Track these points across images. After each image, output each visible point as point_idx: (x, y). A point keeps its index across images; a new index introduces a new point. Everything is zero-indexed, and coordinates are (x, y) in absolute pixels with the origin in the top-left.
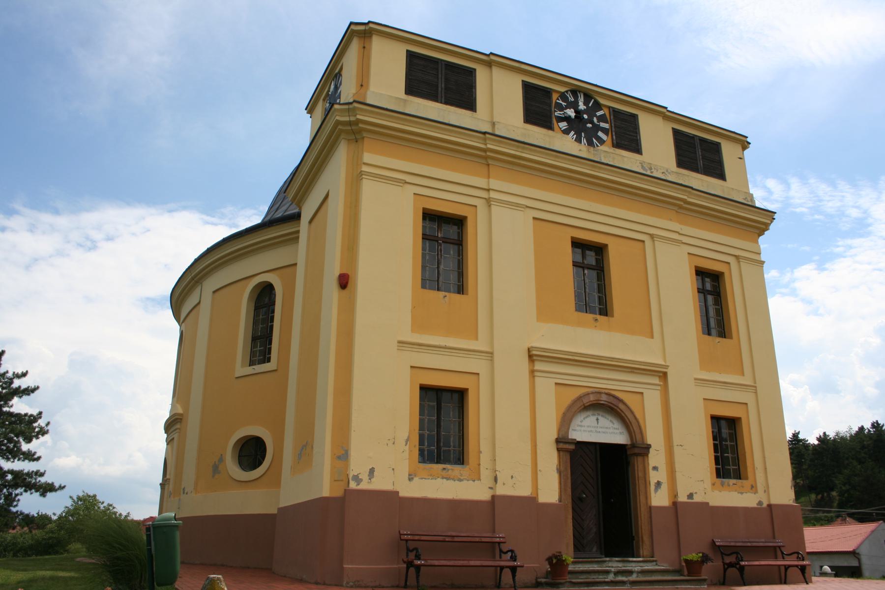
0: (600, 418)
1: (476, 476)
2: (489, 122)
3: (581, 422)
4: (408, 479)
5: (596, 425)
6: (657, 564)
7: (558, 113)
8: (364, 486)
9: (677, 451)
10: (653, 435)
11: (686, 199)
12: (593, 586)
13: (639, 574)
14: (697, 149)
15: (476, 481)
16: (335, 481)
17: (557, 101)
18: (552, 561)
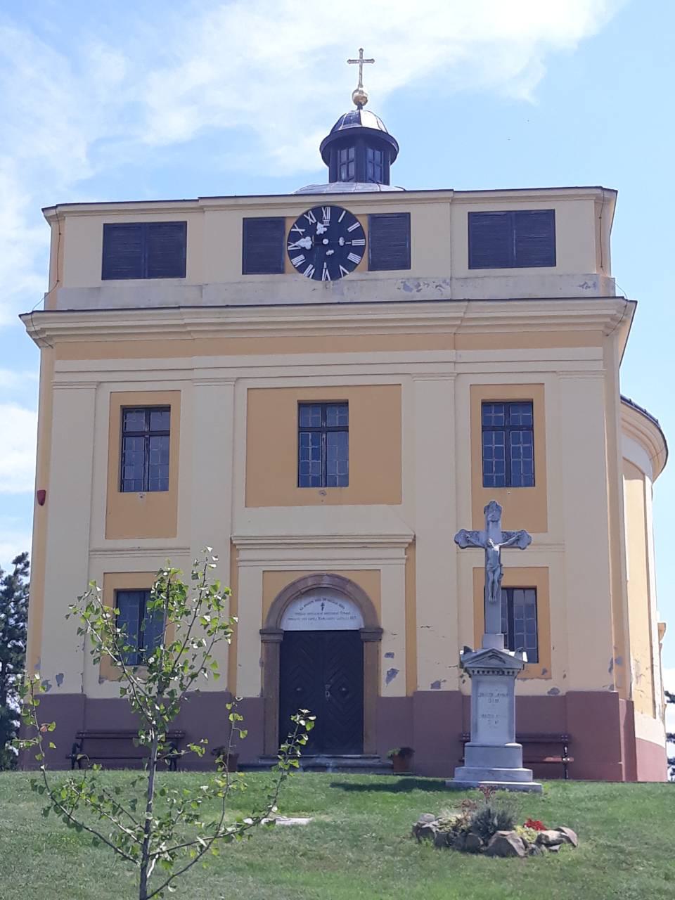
0: (326, 603)
5: (320, 611)
6: (380, 761)
10: (390, 618)
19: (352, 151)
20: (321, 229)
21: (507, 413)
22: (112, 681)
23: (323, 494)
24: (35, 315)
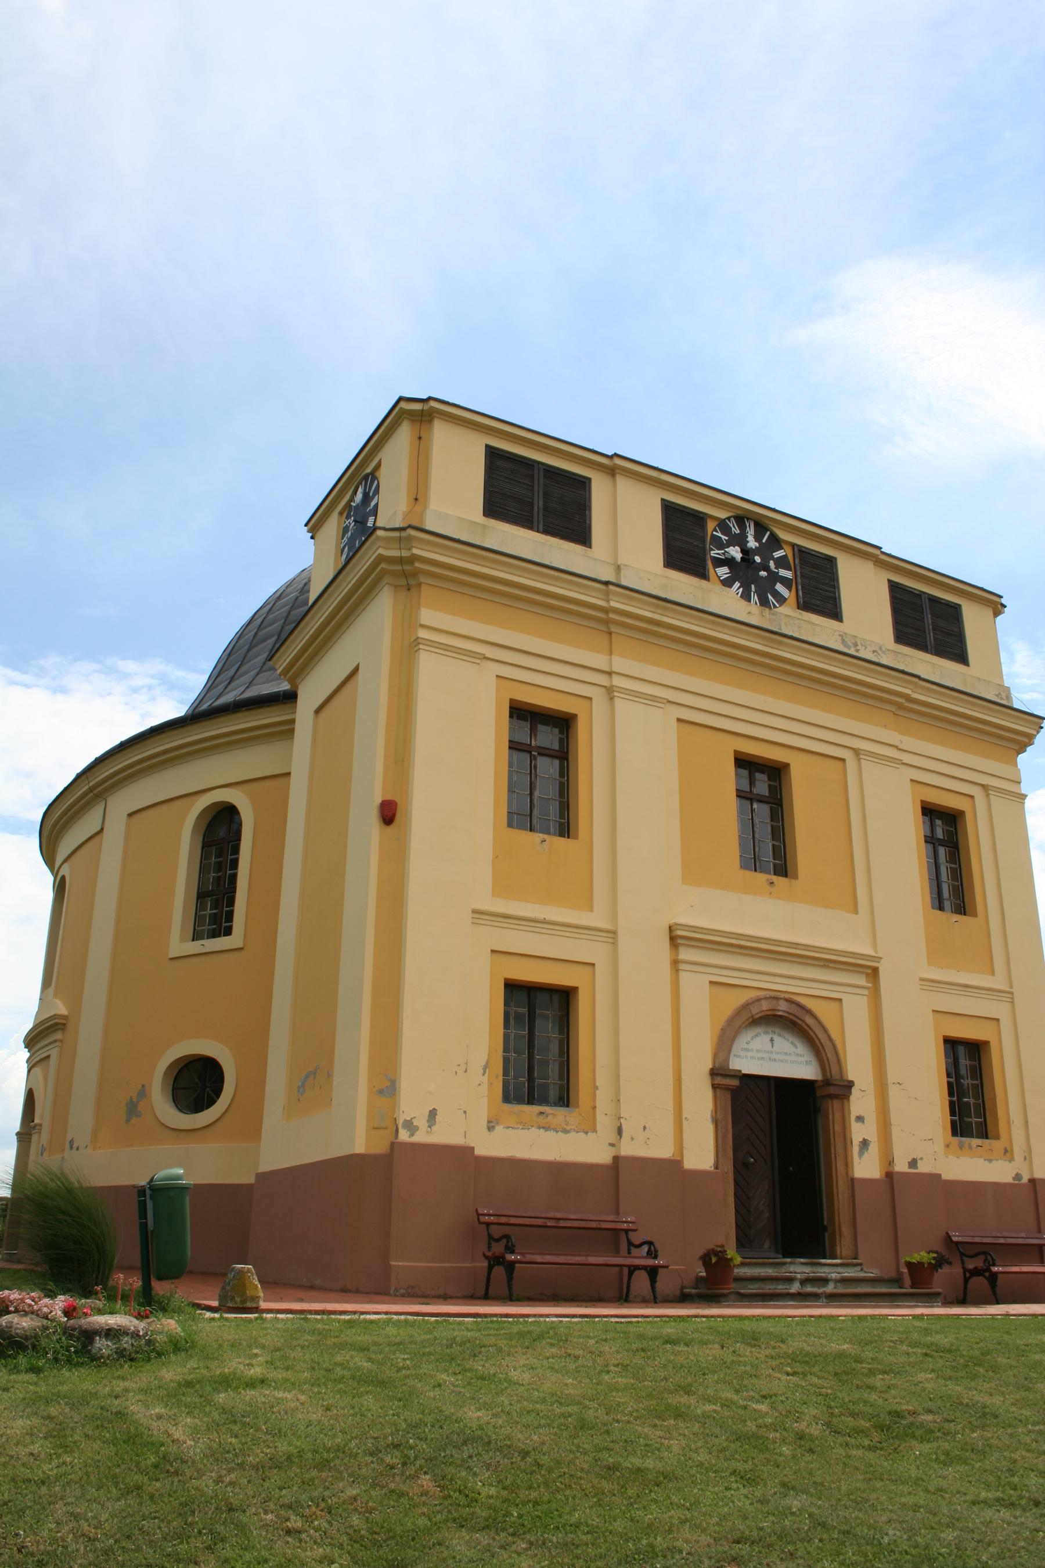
0: (776, 1038)
1: (590, 1127)
2: (612, 564)
3: (747, 1043)
4: (486, 1127)
5: (769, 1048)
6: (862, 1270)
7: (715, 553)
8: (421, 1137)
9: (893, 1091)
11: (909, 695)
12: (770, 1300)
13: (838, 1284)
14: (925, 613)
15: (589, 1134)
16: (374, 1128)
17: (714, 533)
18: (711, 1259)
22: (508, 1128)
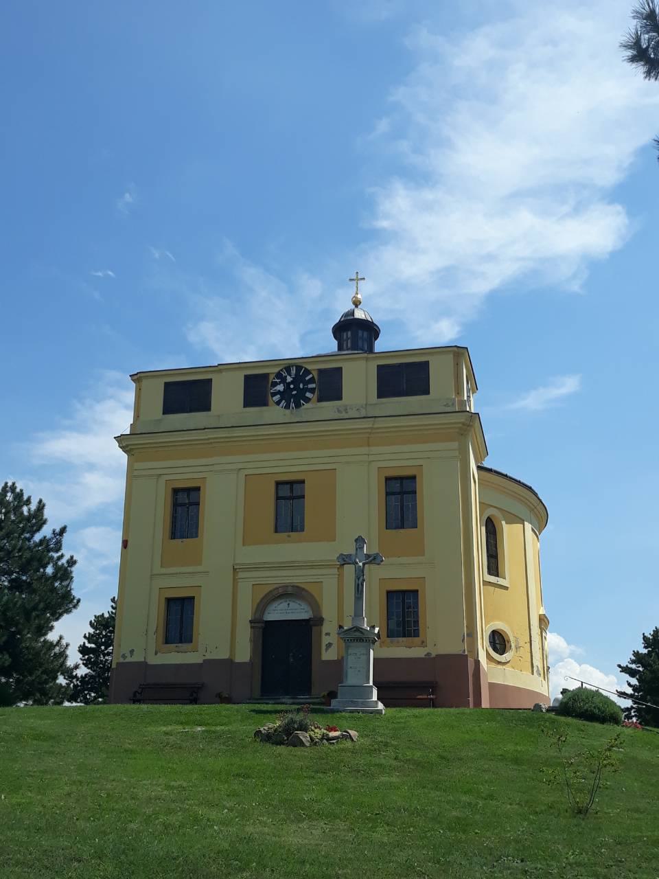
0: (292, 604)
8: (129, 659)
19: (349, 333)
20: (289, 379)
21: (401, 484)
23: (289, 536)
24: (122, 437)
